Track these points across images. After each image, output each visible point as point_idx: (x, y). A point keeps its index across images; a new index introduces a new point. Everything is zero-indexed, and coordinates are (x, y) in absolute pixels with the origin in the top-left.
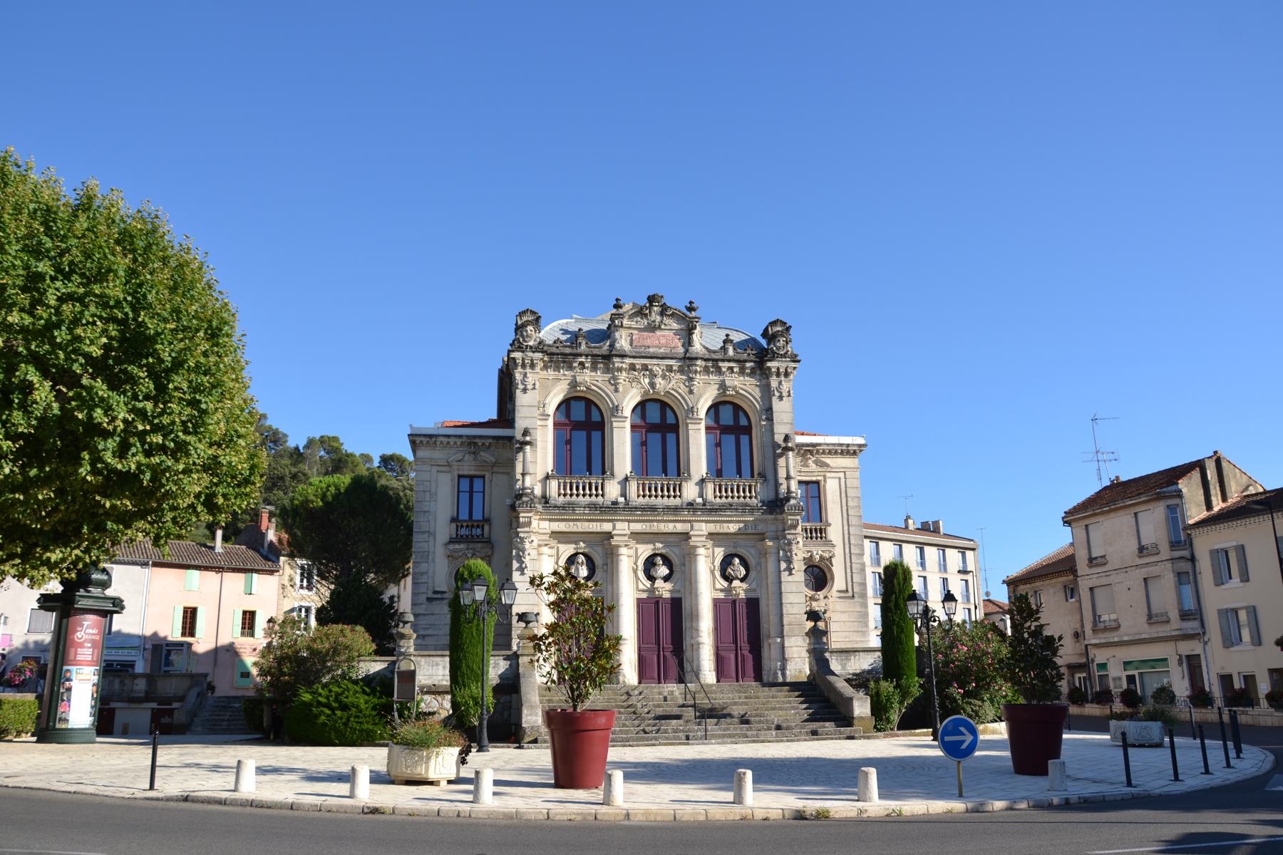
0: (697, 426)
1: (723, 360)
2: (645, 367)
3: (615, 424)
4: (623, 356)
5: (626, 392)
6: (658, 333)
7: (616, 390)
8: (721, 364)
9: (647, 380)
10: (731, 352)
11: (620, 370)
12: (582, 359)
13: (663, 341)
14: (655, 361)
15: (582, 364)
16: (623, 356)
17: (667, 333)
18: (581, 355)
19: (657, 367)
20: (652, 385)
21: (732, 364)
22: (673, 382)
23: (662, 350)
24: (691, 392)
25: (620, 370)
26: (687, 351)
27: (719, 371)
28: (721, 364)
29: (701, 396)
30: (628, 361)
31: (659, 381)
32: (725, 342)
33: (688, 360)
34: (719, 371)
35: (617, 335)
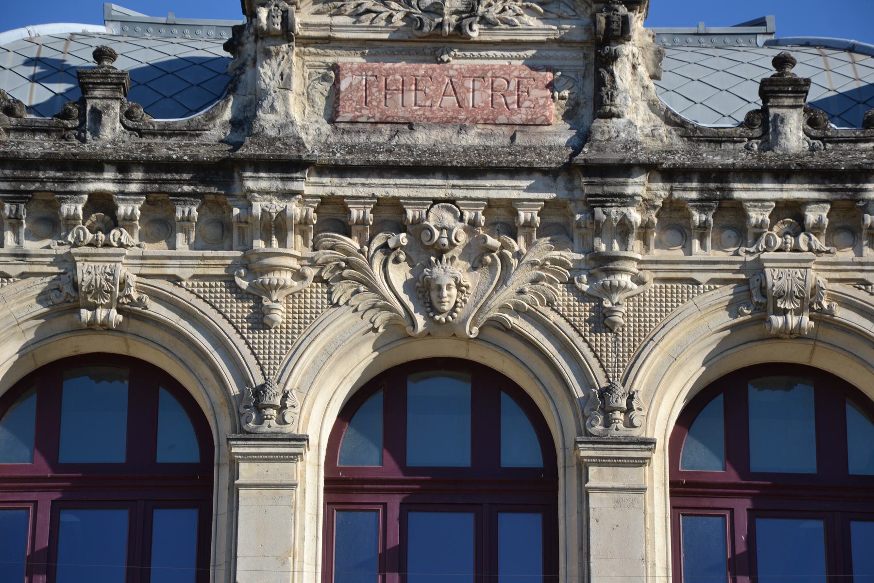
0: (627, 476)
1: (752, 174)
2: (390, 215)
3: (247, 472)
4: (288, 164)
5: (303, 324)
6: (458, 62)
7: (260, 321)
8: (741, 191)
9: (399, 275)
10: (794, 135)
11: (277, 227)
12: (105, 183)
13: (478, 97)
14: (436, 187)
15: (102, 204)
16: (288, 164)
17: (495, 60)
18: (96, 165)
19: (447, 211)
20: (424, 292)
21: (795, 191)
22: (520, 278)
23: (471, 138)
24: (602, 321)
25: (277, 227)
26: (584, 137)
27: (734, 222)
28: (741, 191)
29: (645, 339)
30: (311, 186)
31: (454, 274)
32: (769, 90)
33: (587, 178)
34: (734, 222)
35: (268, 73)
